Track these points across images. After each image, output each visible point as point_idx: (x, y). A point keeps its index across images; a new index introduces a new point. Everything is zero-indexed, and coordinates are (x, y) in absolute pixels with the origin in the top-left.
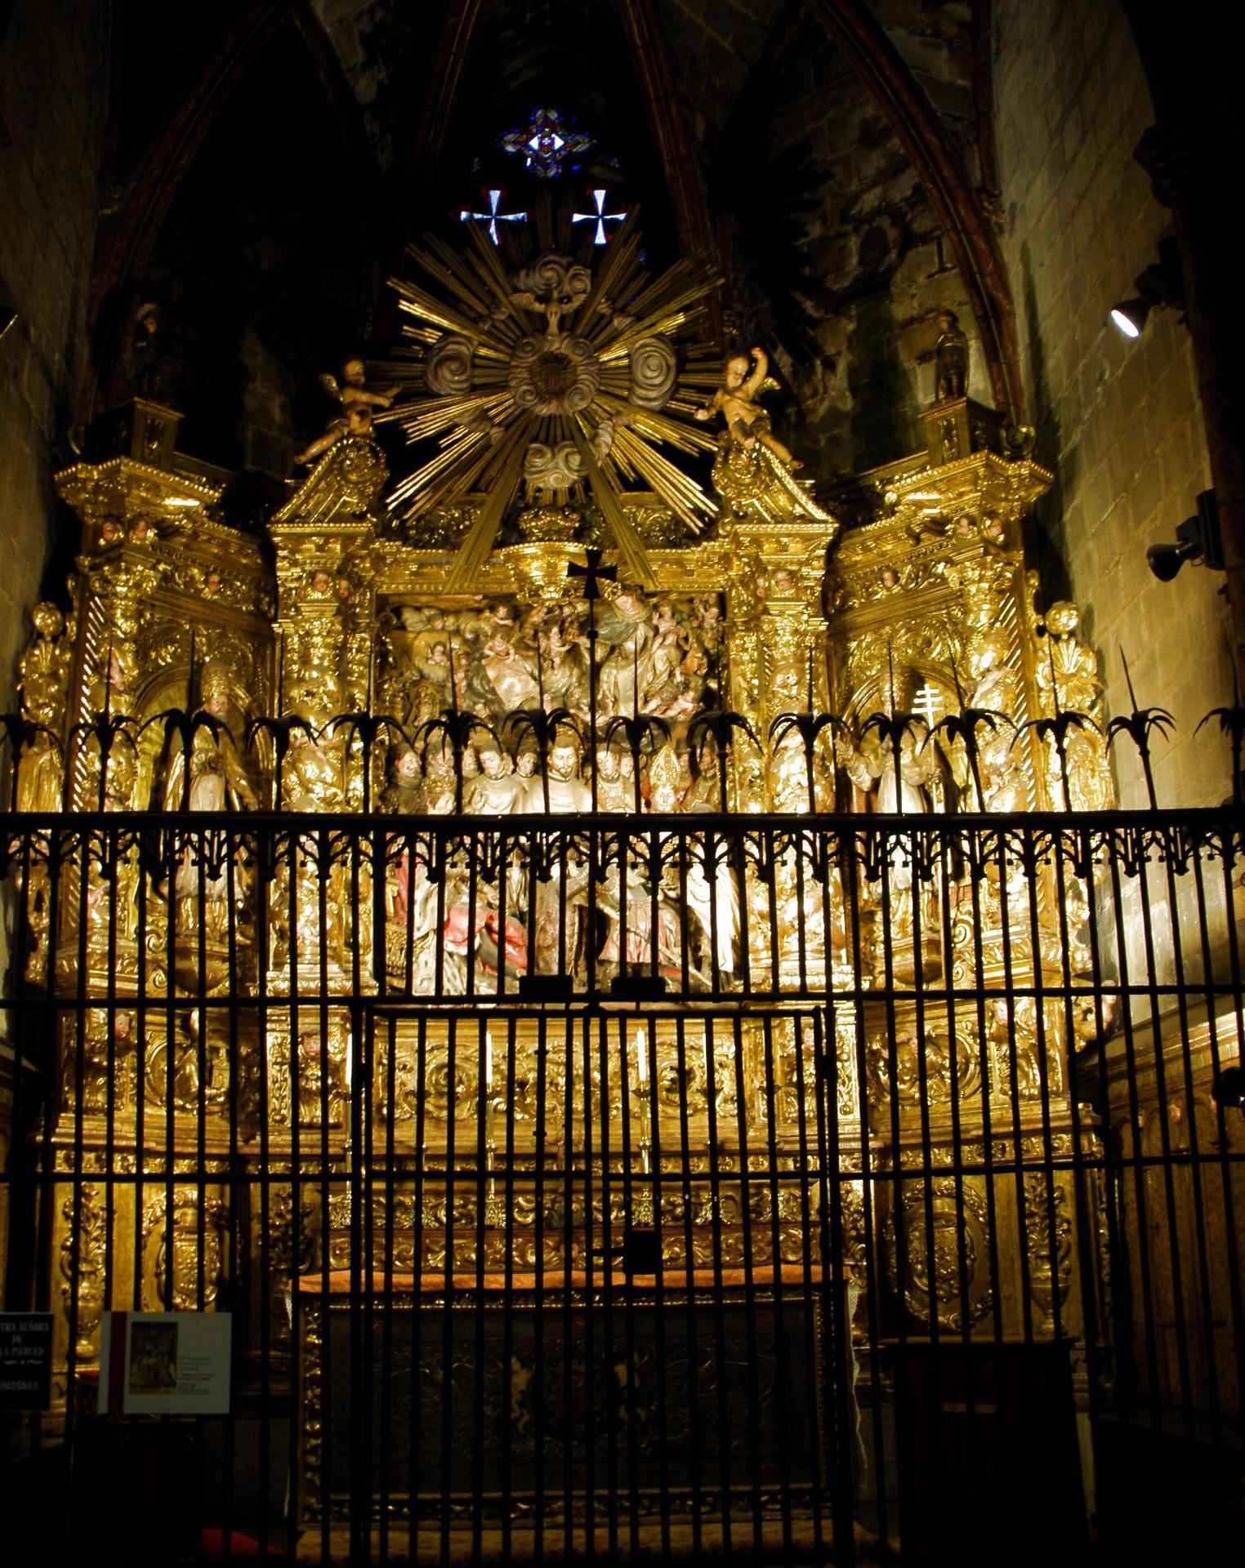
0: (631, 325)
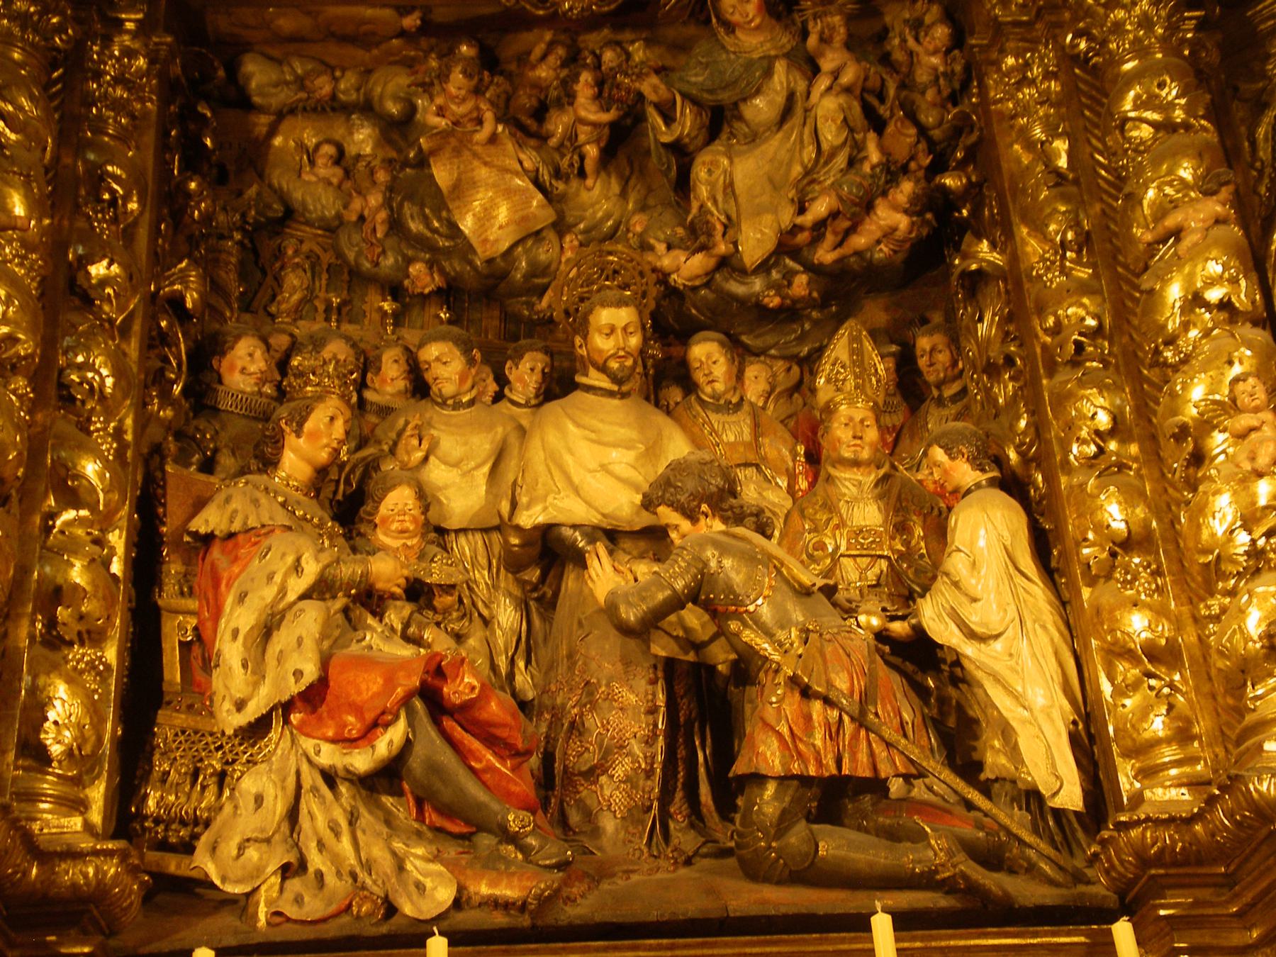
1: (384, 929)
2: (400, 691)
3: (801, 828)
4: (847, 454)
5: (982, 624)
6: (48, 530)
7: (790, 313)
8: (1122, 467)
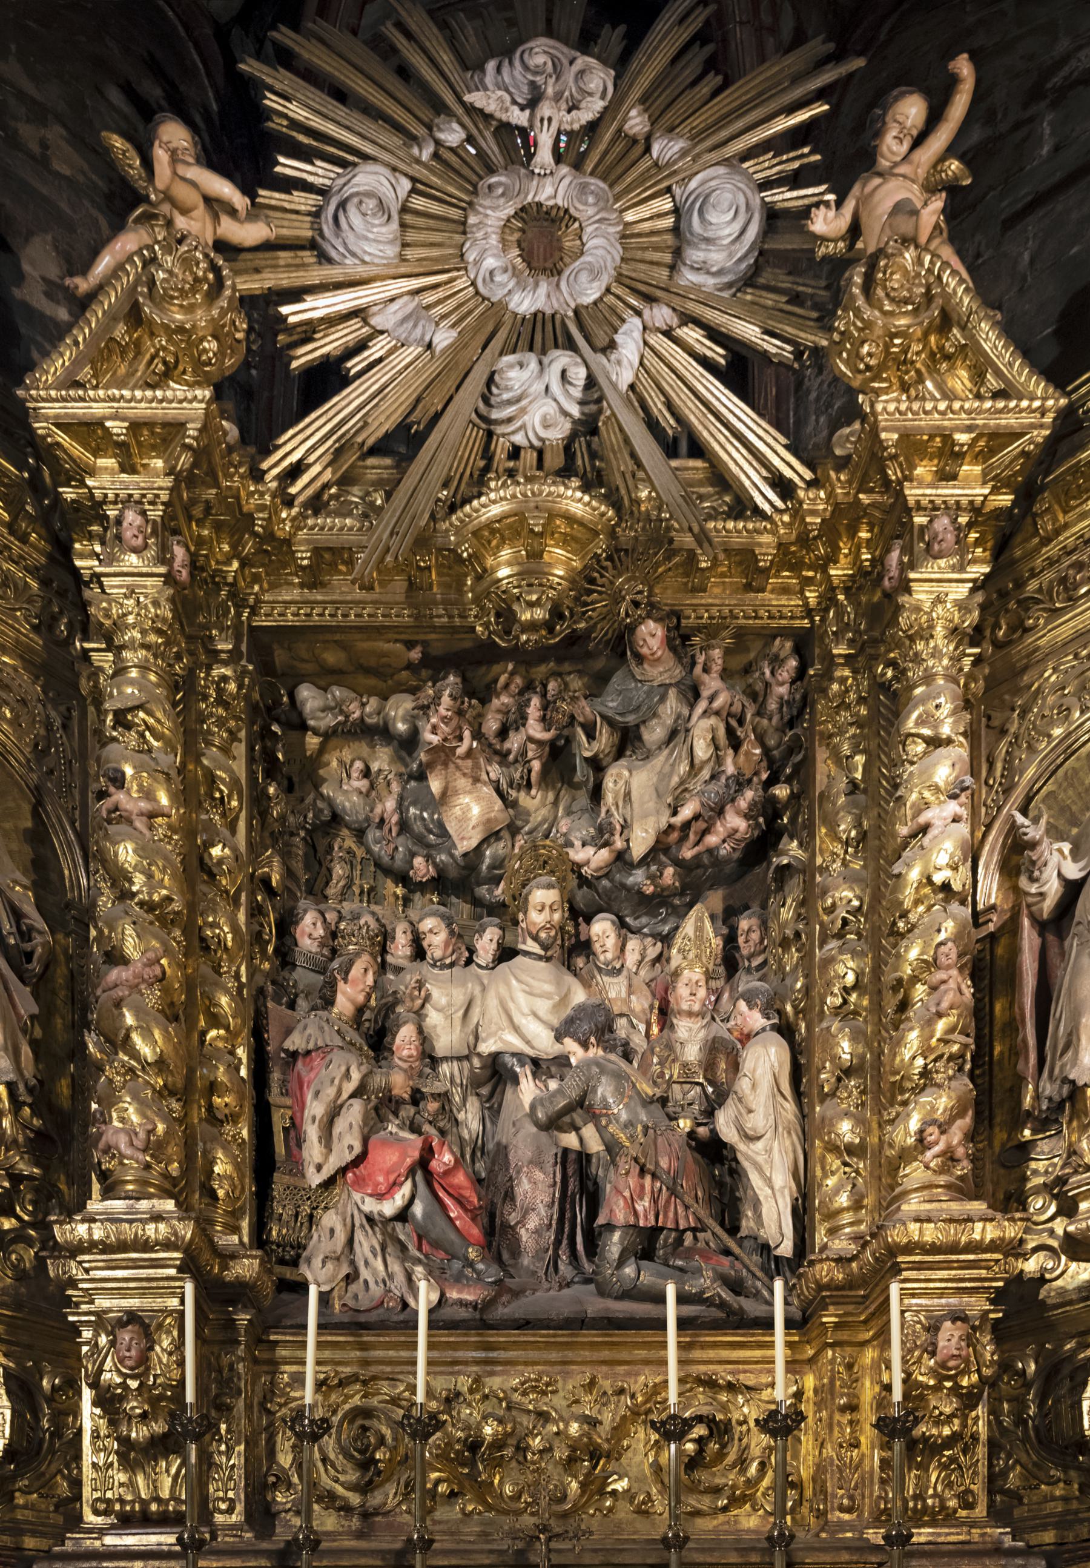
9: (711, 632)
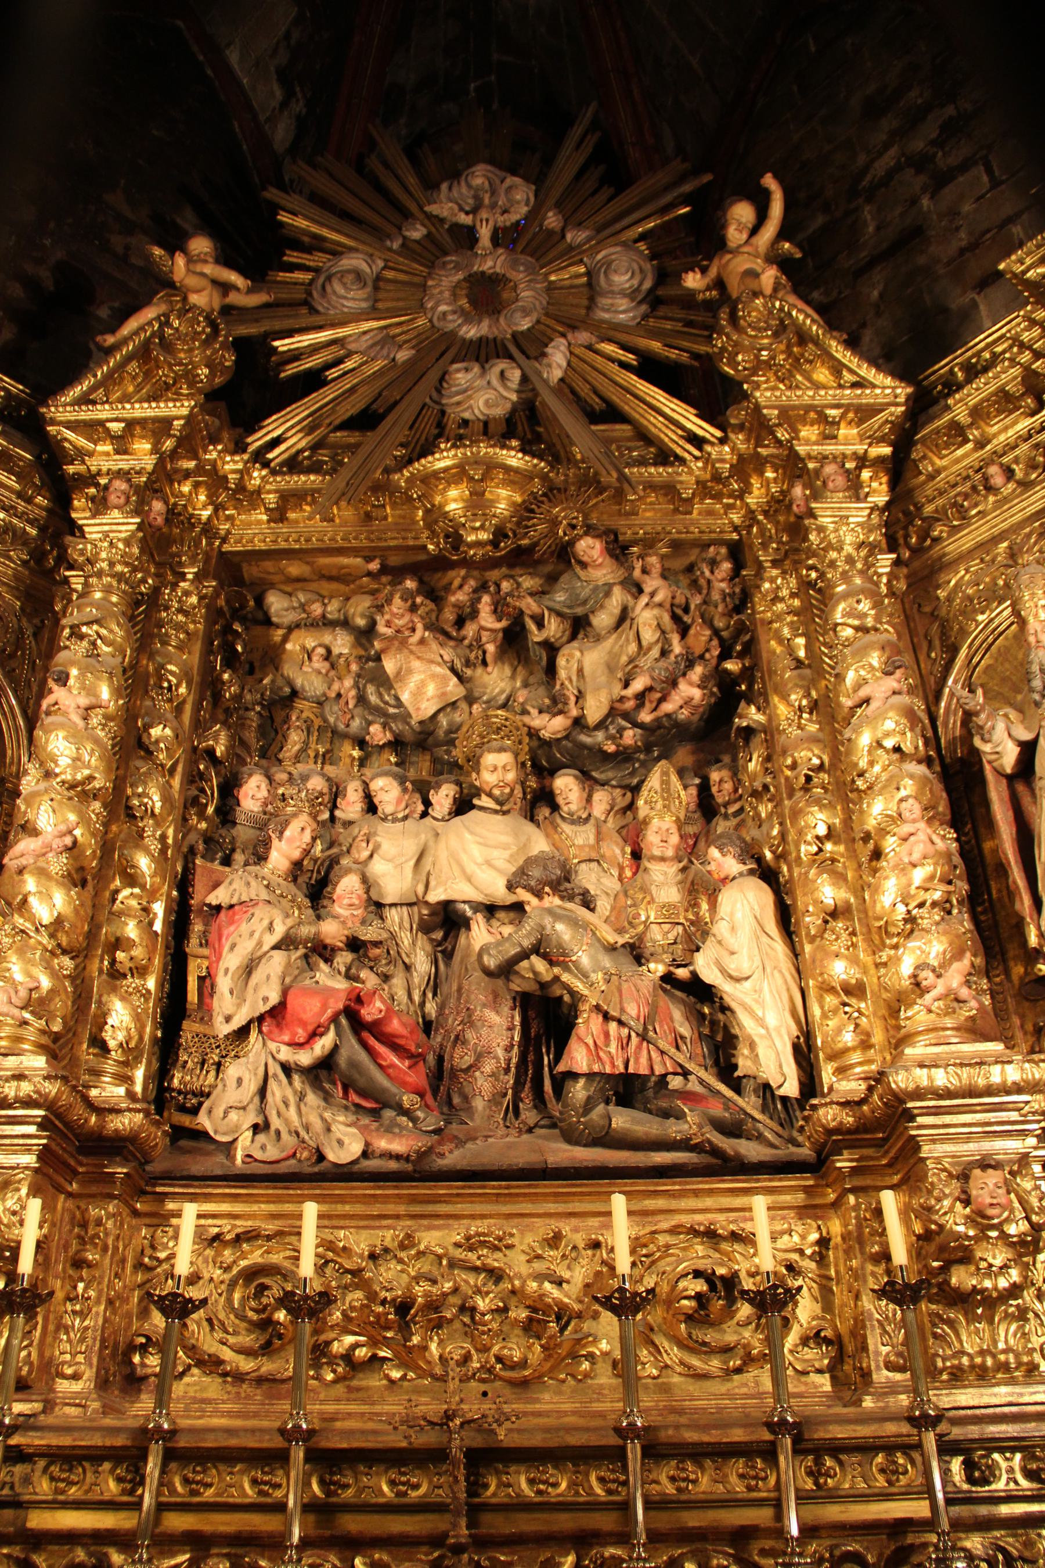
0: (589, 239)
1: (316, 1169)
2: (329, 1012)
3: (600, 1108)
4: (657, 852)
5: (737, 970)
6: (114, 900)
7: (623, 757)
8: (833, 860)
9: (649, 543)
